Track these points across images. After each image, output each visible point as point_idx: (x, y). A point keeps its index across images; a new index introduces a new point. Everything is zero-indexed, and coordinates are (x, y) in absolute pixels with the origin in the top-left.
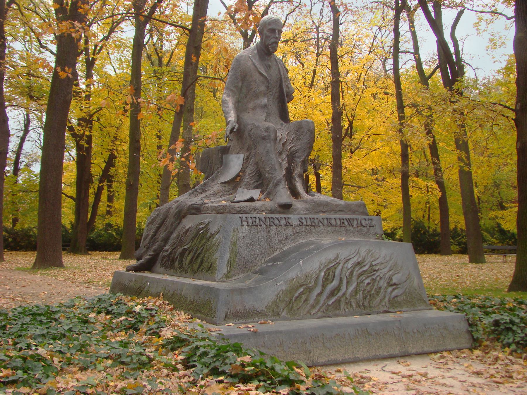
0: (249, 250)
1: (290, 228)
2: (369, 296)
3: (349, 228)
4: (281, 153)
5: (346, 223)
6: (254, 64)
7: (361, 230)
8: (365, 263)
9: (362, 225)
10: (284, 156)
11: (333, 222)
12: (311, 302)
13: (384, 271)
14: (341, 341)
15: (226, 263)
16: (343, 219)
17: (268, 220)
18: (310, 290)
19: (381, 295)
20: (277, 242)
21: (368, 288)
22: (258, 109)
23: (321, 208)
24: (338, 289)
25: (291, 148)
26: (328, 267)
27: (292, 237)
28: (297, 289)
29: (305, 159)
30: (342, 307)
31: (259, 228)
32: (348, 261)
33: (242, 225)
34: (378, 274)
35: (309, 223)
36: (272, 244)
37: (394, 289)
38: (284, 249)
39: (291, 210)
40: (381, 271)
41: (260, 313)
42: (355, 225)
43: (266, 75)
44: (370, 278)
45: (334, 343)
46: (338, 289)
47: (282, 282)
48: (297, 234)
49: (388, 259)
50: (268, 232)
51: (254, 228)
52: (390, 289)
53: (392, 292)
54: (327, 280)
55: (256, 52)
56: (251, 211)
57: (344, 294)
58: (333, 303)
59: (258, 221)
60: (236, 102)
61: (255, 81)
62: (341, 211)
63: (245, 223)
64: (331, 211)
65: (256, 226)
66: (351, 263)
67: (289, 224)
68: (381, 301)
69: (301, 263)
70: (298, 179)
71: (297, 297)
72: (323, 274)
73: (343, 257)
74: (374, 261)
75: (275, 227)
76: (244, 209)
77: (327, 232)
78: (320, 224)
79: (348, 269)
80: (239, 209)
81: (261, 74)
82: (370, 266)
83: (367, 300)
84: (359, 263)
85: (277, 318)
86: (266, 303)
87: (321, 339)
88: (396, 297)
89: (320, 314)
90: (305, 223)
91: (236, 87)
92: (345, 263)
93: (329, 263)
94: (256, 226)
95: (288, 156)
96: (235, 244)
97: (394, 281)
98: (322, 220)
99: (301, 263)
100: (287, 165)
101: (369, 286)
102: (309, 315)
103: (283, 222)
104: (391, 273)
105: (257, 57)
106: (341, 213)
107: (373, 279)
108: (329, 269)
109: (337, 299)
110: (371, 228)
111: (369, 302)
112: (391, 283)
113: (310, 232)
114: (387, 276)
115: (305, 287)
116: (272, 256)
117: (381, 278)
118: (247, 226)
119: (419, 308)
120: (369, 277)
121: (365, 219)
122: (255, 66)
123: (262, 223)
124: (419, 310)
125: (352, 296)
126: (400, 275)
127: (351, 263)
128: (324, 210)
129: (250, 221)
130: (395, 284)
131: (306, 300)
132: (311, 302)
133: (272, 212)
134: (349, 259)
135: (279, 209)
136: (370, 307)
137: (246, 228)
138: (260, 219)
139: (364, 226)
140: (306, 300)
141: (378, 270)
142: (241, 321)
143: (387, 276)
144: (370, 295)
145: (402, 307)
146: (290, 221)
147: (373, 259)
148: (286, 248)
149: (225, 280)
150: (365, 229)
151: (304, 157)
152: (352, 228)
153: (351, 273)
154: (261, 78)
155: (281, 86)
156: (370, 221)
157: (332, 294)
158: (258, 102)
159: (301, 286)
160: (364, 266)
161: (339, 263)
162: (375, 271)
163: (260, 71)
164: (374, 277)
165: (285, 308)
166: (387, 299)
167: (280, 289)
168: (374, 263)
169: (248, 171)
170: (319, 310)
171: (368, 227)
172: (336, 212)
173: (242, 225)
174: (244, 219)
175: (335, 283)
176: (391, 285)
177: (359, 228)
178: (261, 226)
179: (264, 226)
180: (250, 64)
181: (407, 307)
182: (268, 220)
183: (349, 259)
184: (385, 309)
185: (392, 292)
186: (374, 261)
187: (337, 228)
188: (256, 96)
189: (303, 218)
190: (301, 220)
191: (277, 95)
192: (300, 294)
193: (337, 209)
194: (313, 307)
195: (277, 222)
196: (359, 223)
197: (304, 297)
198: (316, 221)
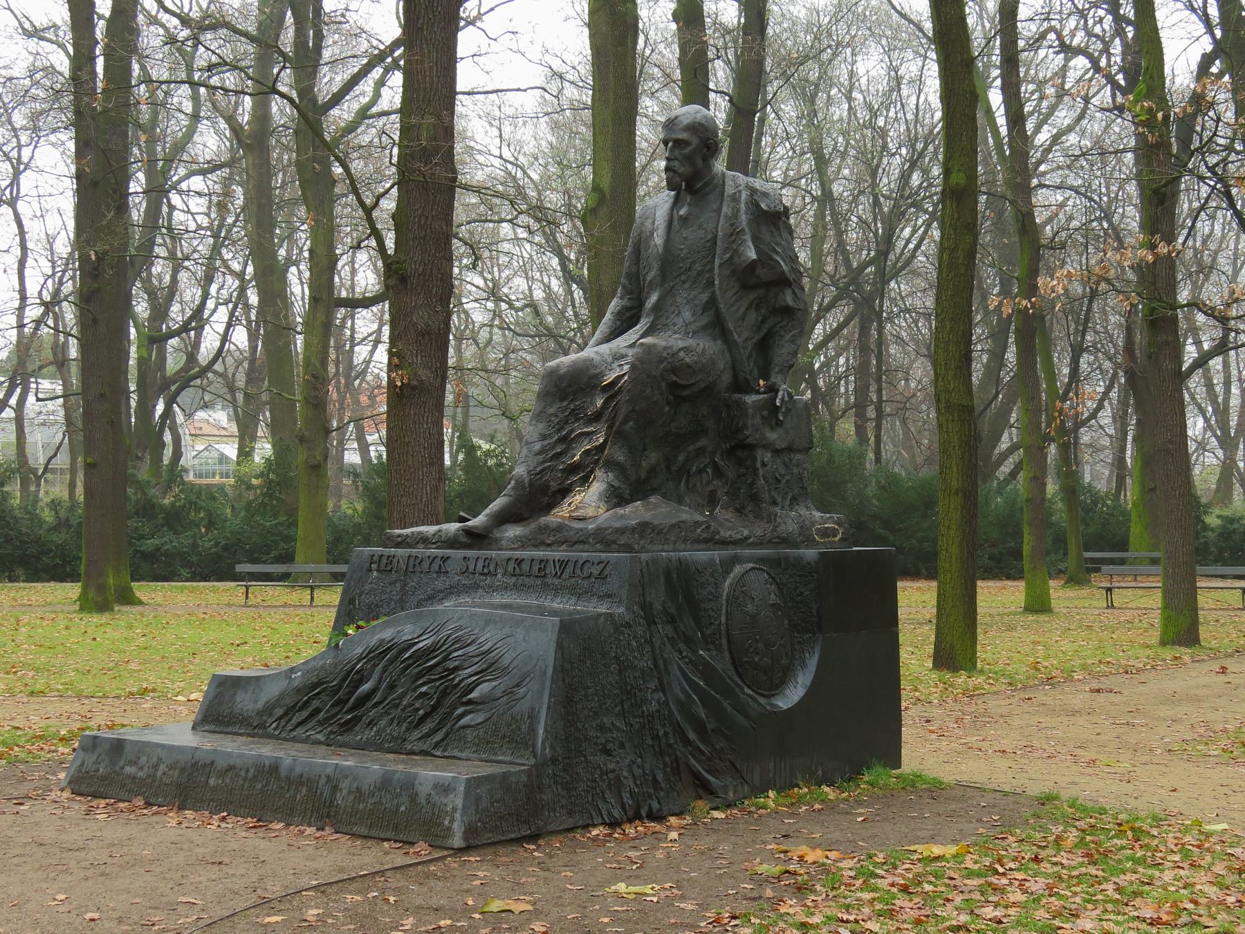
24: (368, 696)
49: (486, 648)
56: (418, 543)
62: (583, 542)
76: (408, 540)
80: (400, 539)
119: (500, 758)
120: (434, 680)
130: (470, 702)
133: (452, 543)
135: (464, 539)
137: (375, 573)
175: (366, 687)
184: (425, 747)
186: (456, 650)
197: (315, 704)
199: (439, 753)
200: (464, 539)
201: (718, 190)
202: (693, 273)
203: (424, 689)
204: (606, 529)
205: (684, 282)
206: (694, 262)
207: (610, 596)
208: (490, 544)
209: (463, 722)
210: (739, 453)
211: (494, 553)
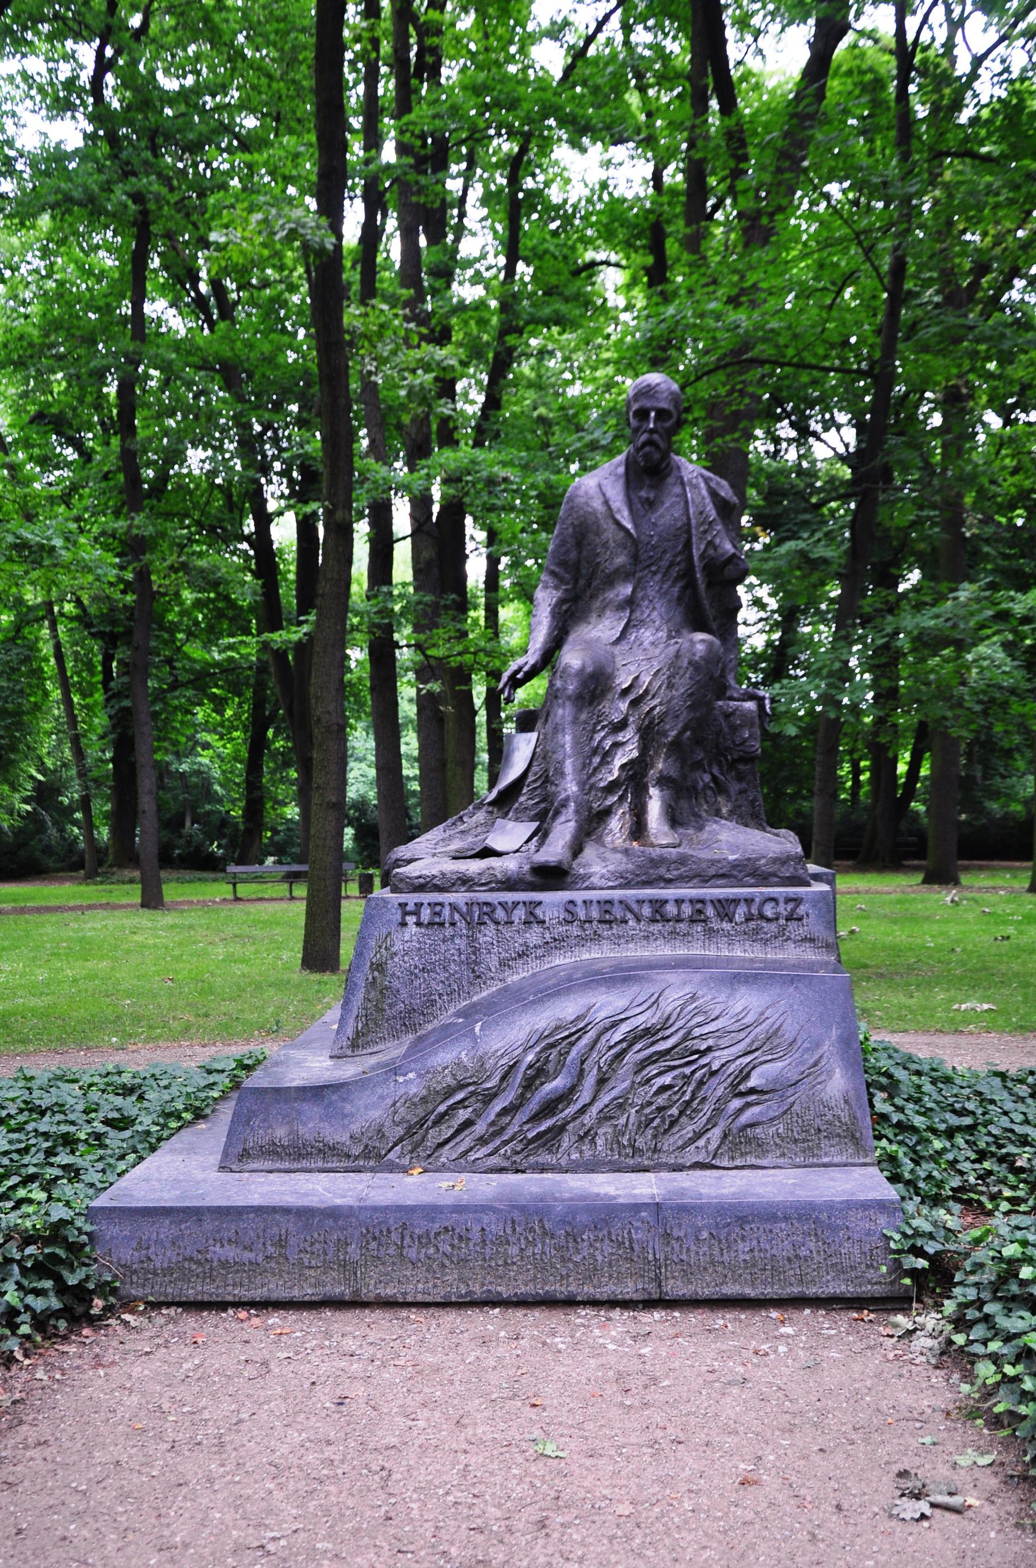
0: (416, 983)
1: (537, 929)
2: (657, 1121)
3: (715, 925)
4: (622, 725)
5: (710, 911)
6: (606, 502)
7: (757, 931)
8: (668, 1032)
9: (762, 917)
10: (629, 734)
11: (671, 909)
12: (480, 1128)
13: (724, 1055)
14: (452, 1246)
15: (355, 1013)
16: (702, 901)
17: (476, 909)
18: (489, 1097)
19: (701, 1120)
20: (494, 962)
21: (661, 1101)
22: (608, 613)
23: (662, 871)
24: (566, 1096)
25: (653, 709)
26: (551, 1040)
27: (540, 952)
28: (450, 1092)
29: (677, 737)
30: (565, 1145)
31: (449, 931)
32: (615, 1025)
33: (404, 924)
34: (704, 1061)
35: (595, 914)
36: (482, 968)
37: (748, 1105)
38: (509, 981)
39: (569, 879)
40: (717, 1054)
41: (332, 1148)
42: (739, 918)
43: (629, 526)
44: (676, 1072)
45: (432, 1251)
46: (566, 1096)
47: (411, 1075)
48: (557, 944)
49: (748, 1020)
50: (472, 939)
51: (437, 934)
52: (736, 1103)
53: (740, 1111)
54: (538, 1074)
55: (621, 470)
57: (583, 1111)
58: (539, 1136)
59: (446, 912)
60: (561, 602)
61: (605, 545)
62: (723, 876)
63: (411, 920)
64: (691, 878)
65: (442, 924)
66: (624, 1028)
67: (532, 919)
68: (698, 1135)
69: (477, 1029)
70: (653, 791)
71: (446, 1113)
72: (530, 1057)
73: (602, 1014)
74: (699, 1025)
75: (492, 926)
76: (435, 881)
77: (646, 938)
78: (629, 916)
79: (611, 1048)
81: (618, 523)
82: (685, 1039)
83: (650, 1132)
84: (647, 1032)
85: (372, 1163)
86: (355, 1128)
87: (394, 1236)
88: (752, 1125)
89: (494, 1161)
90: (582, 914)
91: (563, 564)
92: (607, 1030)
93: (557, 1028)
94: (442, 924)
95: (639, 730)
96: (379, 967)
97: (752, 1083)
98: (634, 906)
99: (477, 1029)
100: (635, 754)
101: (666, 1096)
102: (462, 1164)
103: (520, 914)
104: (748, 1059)
105: (622, 481)
106: (720, 882)
107: (685, 1076)
108: (552, 1046)
109: (554, 1126)
110: (792, 925)
111: (655, 1137)
112: (742, 1088)
113: (597, 937)
114: (732, 1068)
115: (471, 1088)
116: (475, 999)
117: (713, 1074)
118: (418, 924)
119: (826, 1160)
121: (774, 899)
122: (609, 508)
123: (457, 916)
124: (825, 1165)
125: (604, 1117)
126: (780, 1064)
127: (624, 1028)
128: (668, 876)
129: (426, 914)
130: (752, 1091)
131: (468, 1124)
132: (480, 1128)
134: (623, 1020)
136: (655, 1150)
137: (414, 929)
138: (454, 907)
139: (769, 920)
140: (468, 1124)
141: (709, 1049)
142: (278, 1165)
143: (732, 1068)
144: (663, 1120)
145: (765, 1153)
146: (538, 912)
147: (699, 1019)
148: (516, 978)
149: (349, 1052)
150: (772, 927)
151: (674, 733)
152: (726, 926)
153: (620, 1056)
154: (622, 534)
155: (688, 545)
156: (790, 906)
157: (550, 1107)
158: (611, 595)
159: (461, 1086)
160: (664, 1039)
161: (583, 1030)
162: (697, 1052)
163: (618, 517)
164: (687, 1070)
165: (401, 1140)
166: (716, 1134)
167: (402, 1091)
168: (697, 1032)
169: (531, 778)
170: (496, 1151)
171: (782, 922)
172: (705, 880)
173: (404, 924)
174: (411, 907)
176: (741, 1094)
177: (752, 924)
178: (453, 924)
179: (462, 925)
180: (597, 504)
181: (783, 1155)
182: (476, 909)
183: (623, 1020)
184: (700, 1158)
185: (740, 1111)
186: (699, 1025)
187: (682, 927)
188: (611, 580)
189: (579, 902)
190: (571, 907)
191: (675, 571)
192: (453, 1108)
193: (712, 871)
194: (482, 1141)
195: (500, 914)
196: (754, 911)
197: (463, 1115)
198: (618, 912)
199: (725, 1163)
200: (529, 878)
201: (675, 473)
202: (664, 563)
203: (667, 1079)
204: (758, 859)
205: (655, 573)
206: (665, 552)
207: (812, 940)
208: (575, 883)
209: (744, 1118)
210: (741, 767)
211: (579, 896)
